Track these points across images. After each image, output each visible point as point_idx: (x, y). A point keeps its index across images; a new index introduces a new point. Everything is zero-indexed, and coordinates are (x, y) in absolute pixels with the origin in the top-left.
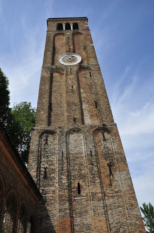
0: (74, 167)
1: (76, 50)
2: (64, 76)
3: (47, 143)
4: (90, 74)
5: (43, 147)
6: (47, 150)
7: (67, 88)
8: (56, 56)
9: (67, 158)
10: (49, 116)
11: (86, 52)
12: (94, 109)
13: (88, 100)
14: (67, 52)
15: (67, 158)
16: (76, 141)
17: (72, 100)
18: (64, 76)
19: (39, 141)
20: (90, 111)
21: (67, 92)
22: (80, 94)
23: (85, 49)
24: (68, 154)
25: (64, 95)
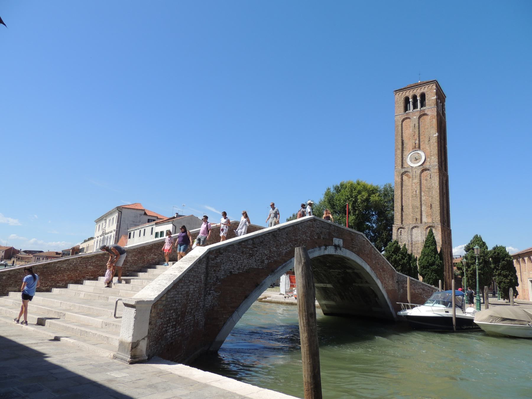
0: (415, 248)
1: (421, 144)
2: (411, 179)
3: (401, 234)
4: (430, 176)
5: (399, 237)
6: (401, 238)
7: (412, 193)
8: (405, 153)
9: (412, 244)
10: (402, 219)
11: (430, 146)
12: (430, 210)
13: (426, 202)
15: (412, 244)
16: (416, 233)
17: (415, 204)
18: (411, 179)
19: (397, 233)
20: (426, 212)
21: (412, 197)
22: (421, 198)
23: (429, 141)
24: (412, 241)
25: (411, 199)
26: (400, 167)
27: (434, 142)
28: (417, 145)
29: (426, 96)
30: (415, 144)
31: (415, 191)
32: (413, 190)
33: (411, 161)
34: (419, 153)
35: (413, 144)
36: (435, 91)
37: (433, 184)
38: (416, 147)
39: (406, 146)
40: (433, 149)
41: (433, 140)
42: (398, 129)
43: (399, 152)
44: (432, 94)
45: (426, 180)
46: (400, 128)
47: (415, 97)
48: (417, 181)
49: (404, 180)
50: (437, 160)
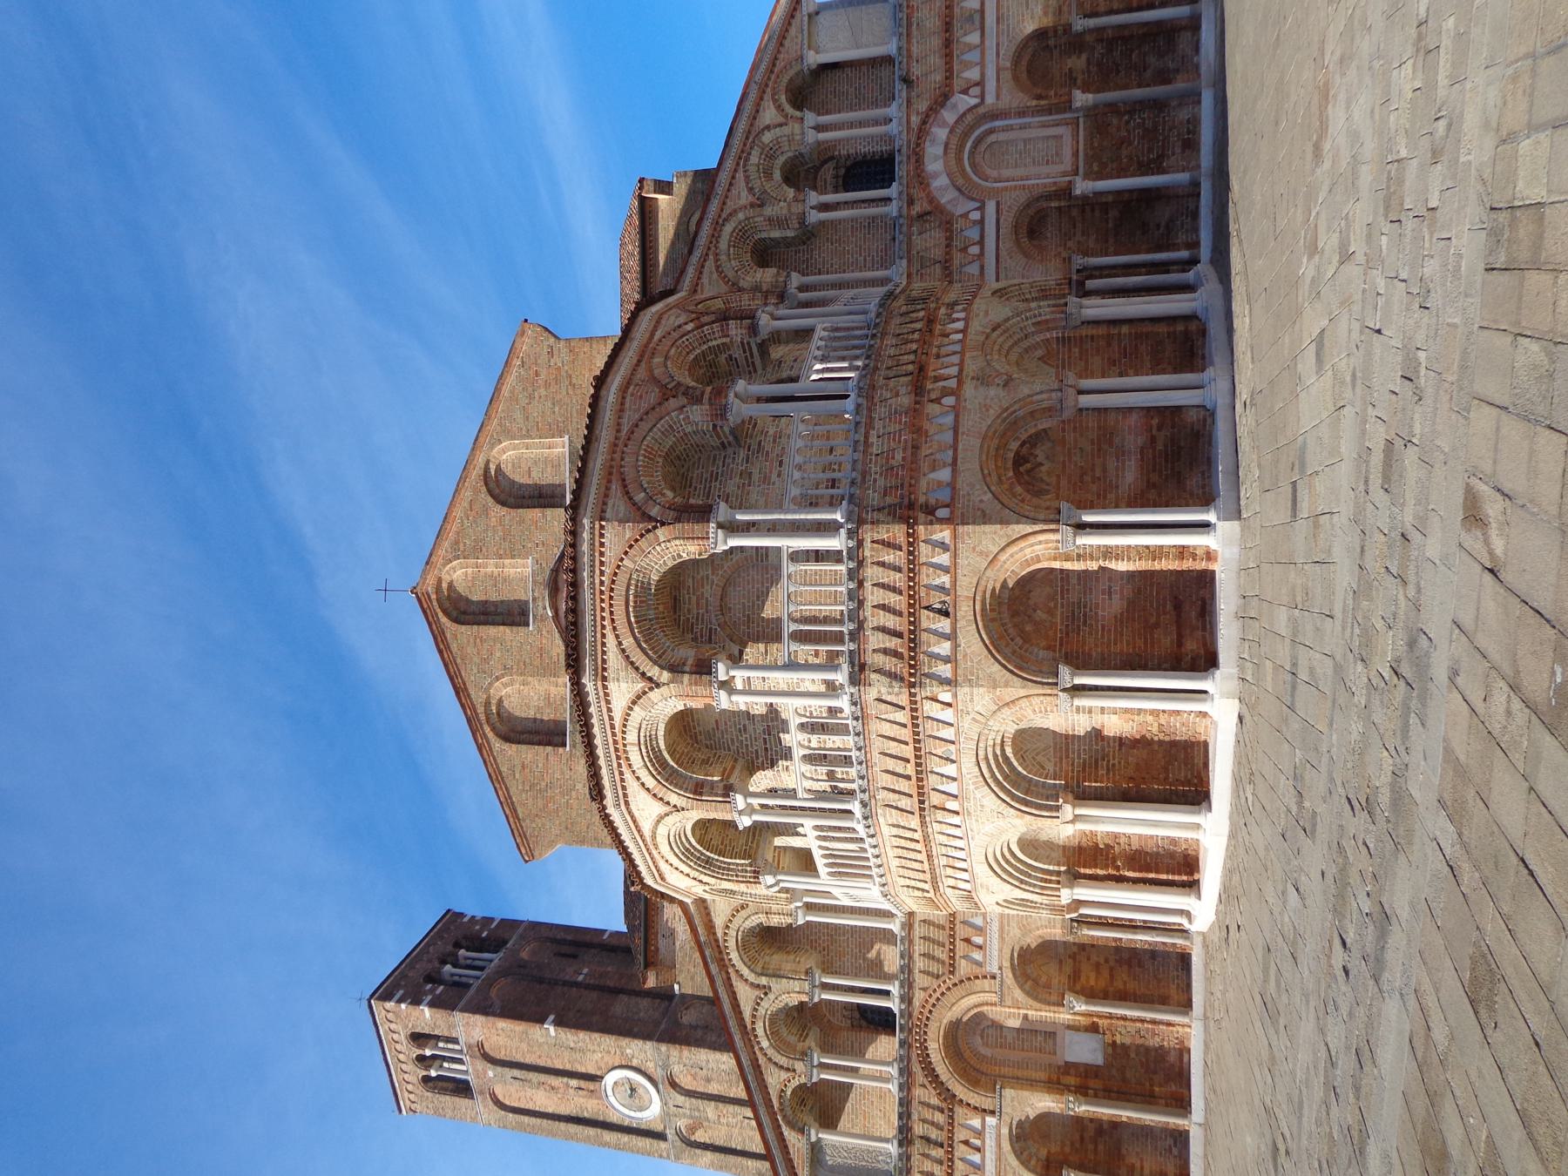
1: (583, 1070)
14: (601, 1098)
18: (705, 1124)
26: (663, 1145)
27: (575, 1038)
28: (583, 1084)
29: (418, 1030)
30: (580, 1089)
31: (746, 1121)
32: (745, 1124)
33: (641, 1109)
34: (615, 1083)
35: (580, 1096)
36: (403, 1006)
37: (723, 1067)
38: (592, 1088)
39: (588, 1111)
40: (599, 1045)
41: (567, 1039)
42: (529, 1125)
43: (609, 1136)
44: (413, 1014)
45: (708, 1080)
46: (526, 1119)
47: (421, 1059)
48: (710, 1110)
49: (708, 1141)
50: (636, 1041)
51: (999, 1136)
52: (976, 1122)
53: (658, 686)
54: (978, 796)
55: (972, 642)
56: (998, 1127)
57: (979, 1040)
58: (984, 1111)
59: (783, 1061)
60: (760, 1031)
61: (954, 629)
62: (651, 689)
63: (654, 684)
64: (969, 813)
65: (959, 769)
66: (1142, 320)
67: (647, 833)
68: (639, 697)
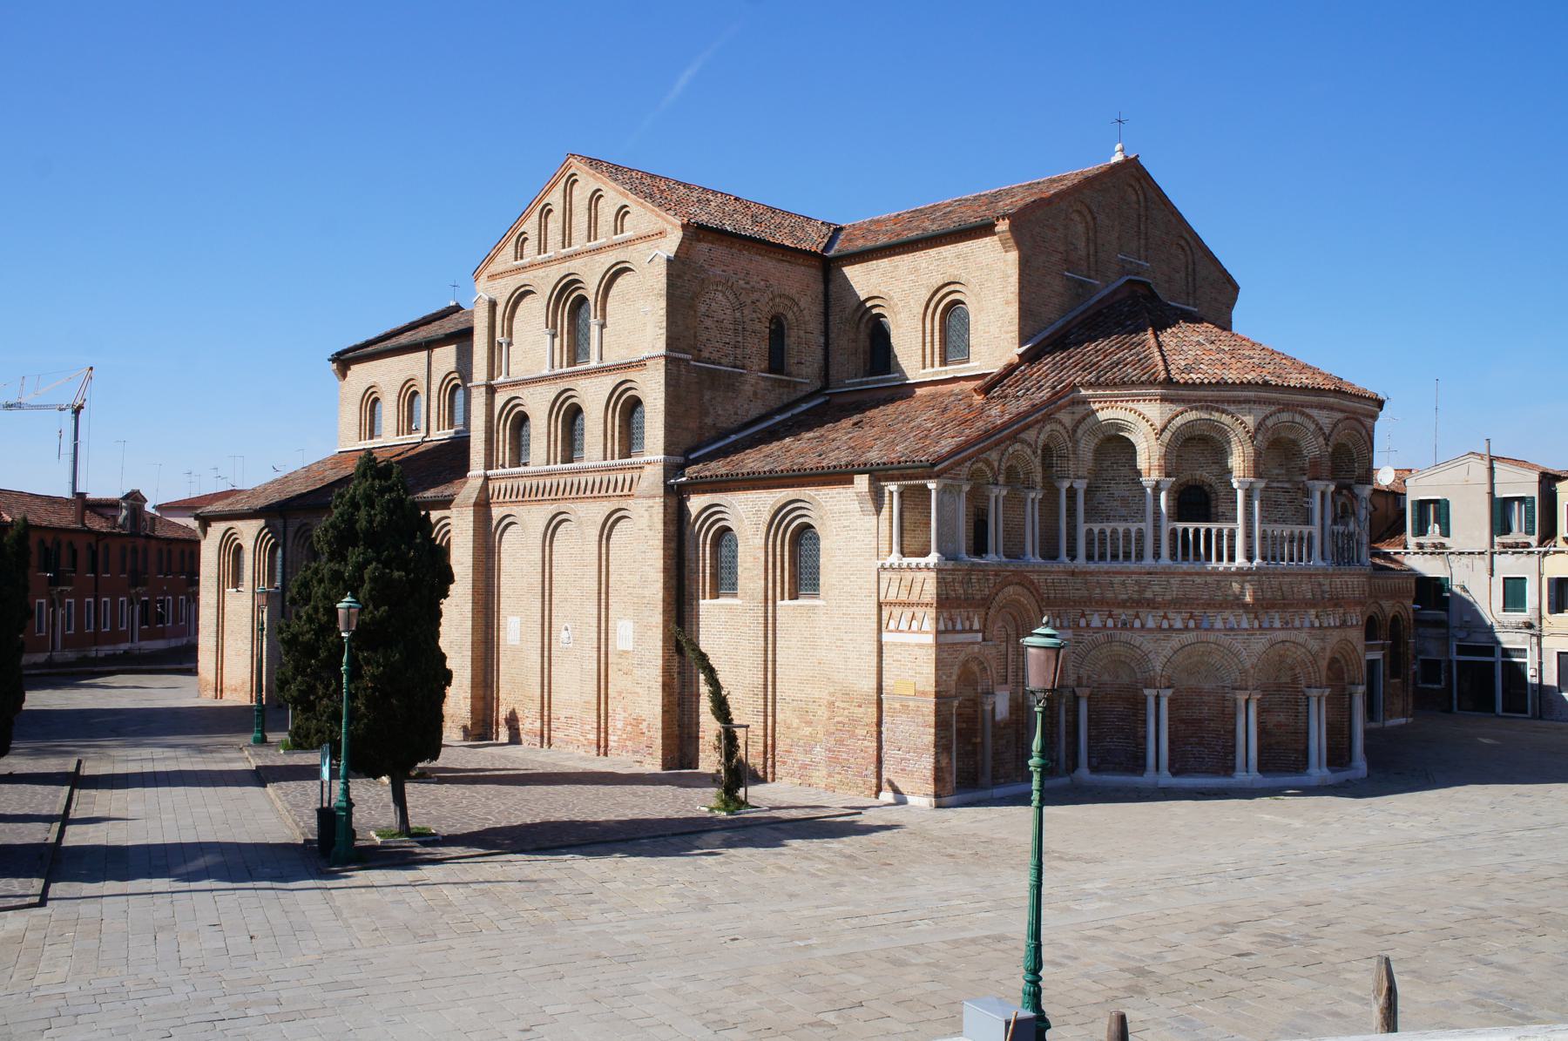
51: (973, 643)
52: (976, 626)
53: (1327, 445)
54: (1263, 641)
55: (1334, 637)
56: (979, 643)
57: (1000, 625)
58: (985, 632)
59: (1003, 466)
60: (1017, 446)
61: (1338, 627)
62: (1325, 439)
63: (1327, 439)
64: (1252, 635)
65: (1279, 629)
66: (1308, 716)
67: (1226, 407)
68: (1321, 429)
